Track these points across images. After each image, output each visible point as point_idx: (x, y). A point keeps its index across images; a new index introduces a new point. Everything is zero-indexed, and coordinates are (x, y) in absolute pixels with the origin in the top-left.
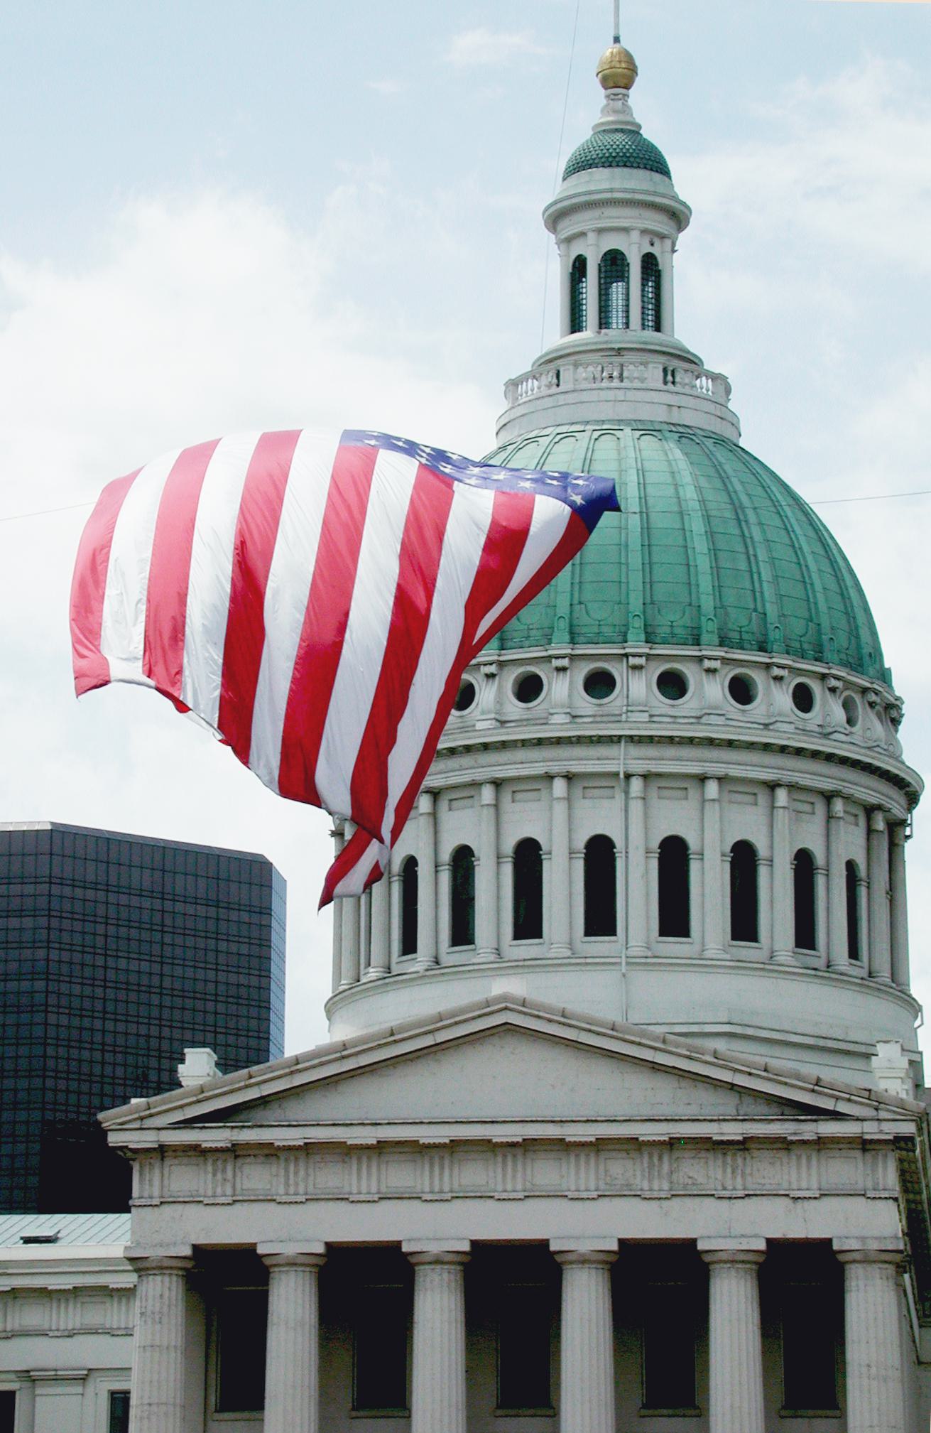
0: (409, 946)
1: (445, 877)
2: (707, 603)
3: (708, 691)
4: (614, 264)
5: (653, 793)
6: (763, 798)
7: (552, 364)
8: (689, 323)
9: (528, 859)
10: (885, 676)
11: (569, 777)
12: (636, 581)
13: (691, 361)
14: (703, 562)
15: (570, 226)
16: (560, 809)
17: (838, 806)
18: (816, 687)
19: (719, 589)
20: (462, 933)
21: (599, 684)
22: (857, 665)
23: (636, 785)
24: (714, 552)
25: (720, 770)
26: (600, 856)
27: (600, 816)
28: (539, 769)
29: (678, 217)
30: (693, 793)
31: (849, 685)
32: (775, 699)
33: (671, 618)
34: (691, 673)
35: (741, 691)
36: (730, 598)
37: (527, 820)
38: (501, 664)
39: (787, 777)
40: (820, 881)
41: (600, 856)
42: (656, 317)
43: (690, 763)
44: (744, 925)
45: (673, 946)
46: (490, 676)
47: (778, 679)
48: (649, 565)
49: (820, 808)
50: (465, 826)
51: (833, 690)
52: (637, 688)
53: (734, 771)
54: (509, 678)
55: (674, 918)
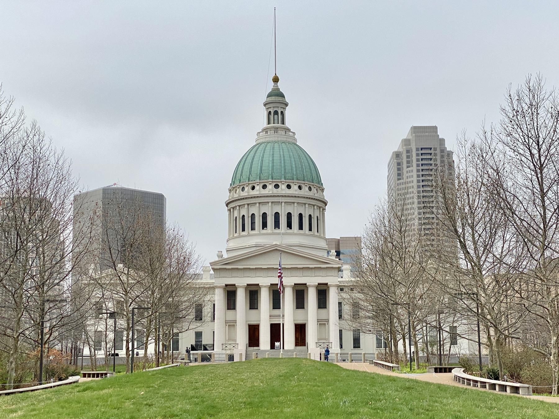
0: (243, 230)
1: (250, 218)
2: (295, 173)
3: (295, 188)
4: (276, 113)
6: (304, 206)
7: (265, 130)
8: (288, 123)
9: (264, 216)
10: (322, 184)
12: (283, 169)
13: (289, 130)
14: (294, 166)
15: (268, 106)
16: (270, 208)
17: (316, 207)
18: (312, 187)
19: (296, 170)
20: (253, 229)
21: (277, 186)
22: (319, 183)
23: (283, 204)
24: (295, 164)
26: (277, 215)
27: (277, 209)
29: (287, 105)
30: (292, 205)
32: (305, 189)
33: (288, 175)
34: (292, 185)
35: (300, 188)
36: (298, 172)
37: (264, 209)
41: (277, 215)
42: (283, 123)
43: (291, 199)
45: (290, 231)
48: (285, 166)
50: (254, 210)
53: (300, 202)
54: (262, 185)
55: (289, 225)
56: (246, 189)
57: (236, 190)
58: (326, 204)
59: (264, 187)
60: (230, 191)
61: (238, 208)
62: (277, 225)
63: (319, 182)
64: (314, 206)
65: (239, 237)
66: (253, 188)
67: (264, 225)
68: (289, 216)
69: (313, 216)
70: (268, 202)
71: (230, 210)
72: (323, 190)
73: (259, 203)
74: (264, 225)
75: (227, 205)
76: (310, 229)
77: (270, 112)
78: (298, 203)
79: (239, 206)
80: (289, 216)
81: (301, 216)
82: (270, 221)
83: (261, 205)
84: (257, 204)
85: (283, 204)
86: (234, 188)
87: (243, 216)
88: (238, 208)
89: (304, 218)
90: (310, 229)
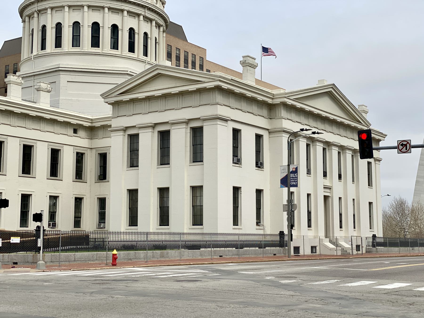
0: (43, 47)
1: (54, 30)
5: (110, 13)
6: (137, 18)
17: (154, 23)
20: (58, 44)
23: (106, 9)
25: (127, 9)
26: (96, 27)
30: (120, 14)
37: (76, 16)
39: (143, 14)
40: (149, 41)
41: (96, 27)
44: (132, 49)
45: (114, 52)
49: (149, 24)
55: (115, 45)
61: (36, 15)
62: (95, 43)
64: (151, 20)
65: (38, 57)
67: (76, 41)
68: (115, 28)
69: (149, 36)
71: (24, 21)
72: (163, 3)
74: (76, 41)
75: (21, 17)
76: (146, 54)
78: (128, 12)
79: (39, 11)
80: (115, 28)
81: (132, 31)
82: (86, 34)
83: (71, 10)
87: (44, 27)
88: (36, 15)
89: (136, 36)
90: (146, 54)
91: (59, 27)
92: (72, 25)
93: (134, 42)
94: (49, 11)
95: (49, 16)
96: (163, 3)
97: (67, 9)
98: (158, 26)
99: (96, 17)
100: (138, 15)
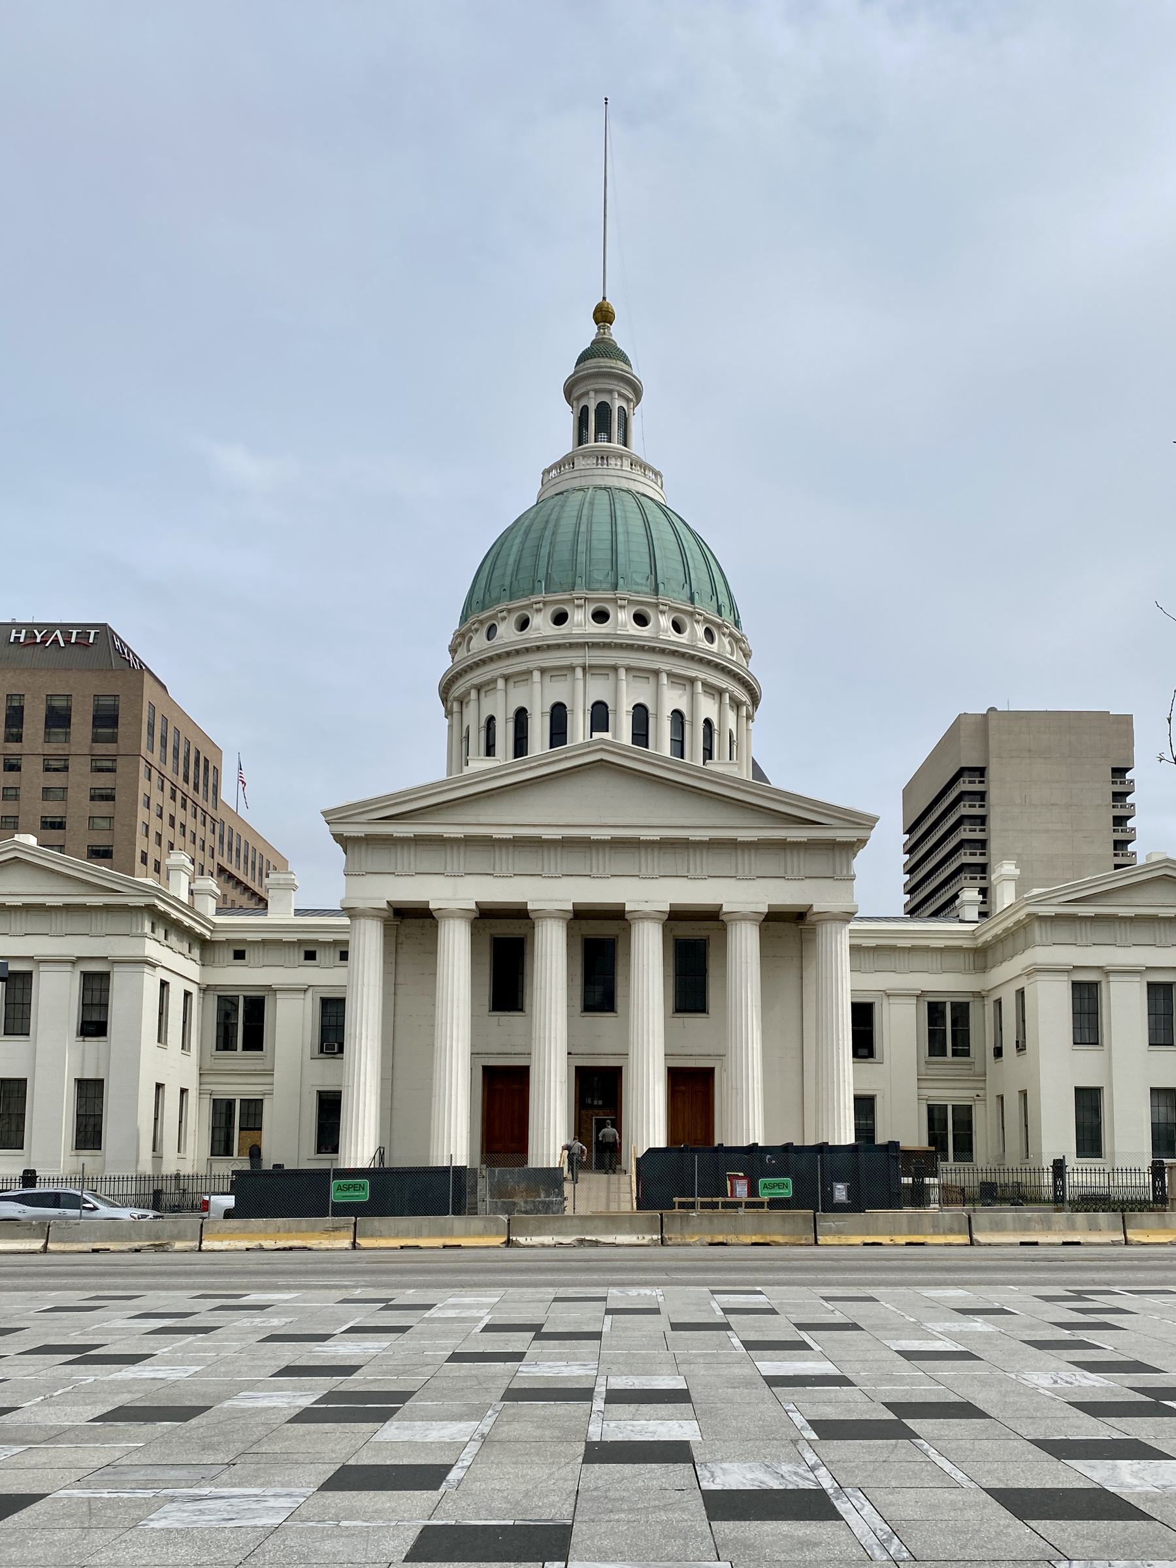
9: (559, 716)
11: (584, 668)
16: (580, 684)
21: (601, 616)
23: (622, 672)
28: (566, 662)
31: (731, 635)
34: (651, 613)
37: (557, 692)
38: (545, 603)
39: (702, 676)
40: (716, 737)
46: (539, 610)
47: (698, 622)
49: (717, 697)
51: (724, 634)
52: (622, 621)
54: (549, 612)
56: (501, 629)
57: (471, 638)
58: (755, 700)
59: (560, 618)
60: (453, 650)
63: (737, 623)
64: (720, 692)
66: (524, 624)
69: (716, 726)
70: (572, 668)
73: (543, 671)
77: (585, 411)
78: (670, 675)
81: (677, 714)
83: (547, 678)
84: (536, 675)
85: (622, 672)
86: (463, 635)
91: (521, 718)
92: (548, 709)
93: (682, 742)
94: (501, 683)
95: (500, 695)
96: (747, 655)
97: (536, 675)
98: (737, 704)
99: (598, 690)
100: (692, 681)
